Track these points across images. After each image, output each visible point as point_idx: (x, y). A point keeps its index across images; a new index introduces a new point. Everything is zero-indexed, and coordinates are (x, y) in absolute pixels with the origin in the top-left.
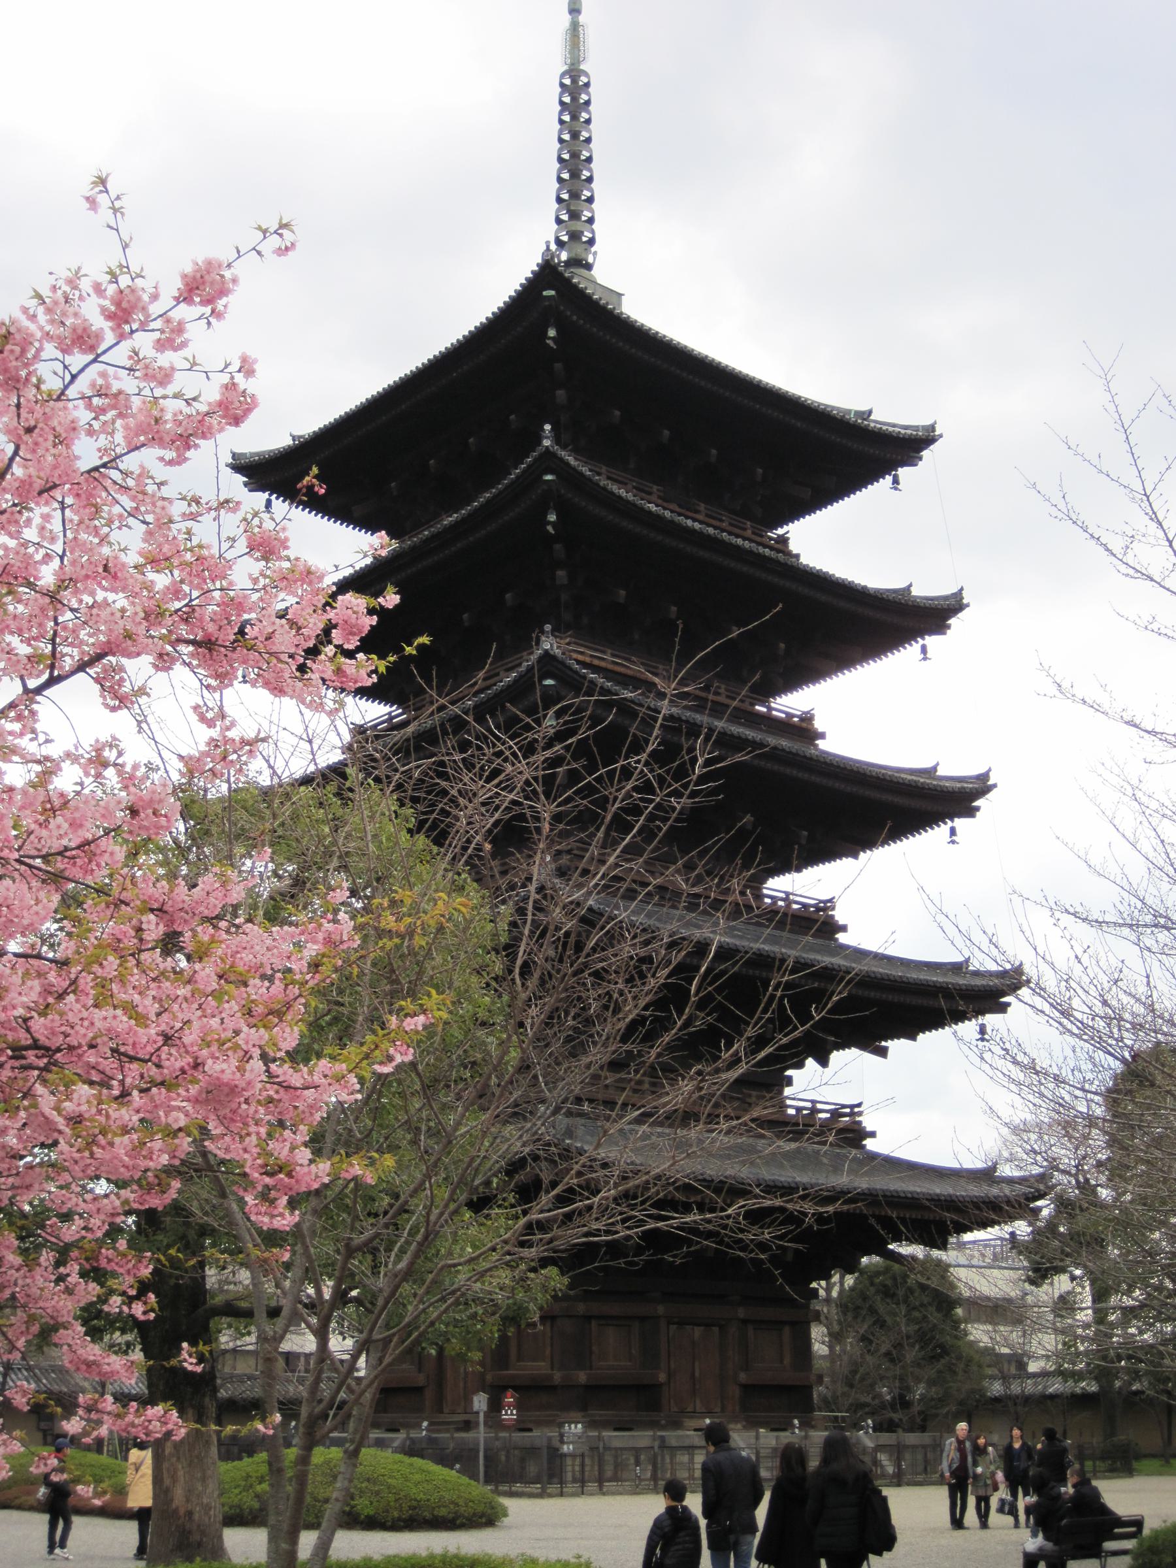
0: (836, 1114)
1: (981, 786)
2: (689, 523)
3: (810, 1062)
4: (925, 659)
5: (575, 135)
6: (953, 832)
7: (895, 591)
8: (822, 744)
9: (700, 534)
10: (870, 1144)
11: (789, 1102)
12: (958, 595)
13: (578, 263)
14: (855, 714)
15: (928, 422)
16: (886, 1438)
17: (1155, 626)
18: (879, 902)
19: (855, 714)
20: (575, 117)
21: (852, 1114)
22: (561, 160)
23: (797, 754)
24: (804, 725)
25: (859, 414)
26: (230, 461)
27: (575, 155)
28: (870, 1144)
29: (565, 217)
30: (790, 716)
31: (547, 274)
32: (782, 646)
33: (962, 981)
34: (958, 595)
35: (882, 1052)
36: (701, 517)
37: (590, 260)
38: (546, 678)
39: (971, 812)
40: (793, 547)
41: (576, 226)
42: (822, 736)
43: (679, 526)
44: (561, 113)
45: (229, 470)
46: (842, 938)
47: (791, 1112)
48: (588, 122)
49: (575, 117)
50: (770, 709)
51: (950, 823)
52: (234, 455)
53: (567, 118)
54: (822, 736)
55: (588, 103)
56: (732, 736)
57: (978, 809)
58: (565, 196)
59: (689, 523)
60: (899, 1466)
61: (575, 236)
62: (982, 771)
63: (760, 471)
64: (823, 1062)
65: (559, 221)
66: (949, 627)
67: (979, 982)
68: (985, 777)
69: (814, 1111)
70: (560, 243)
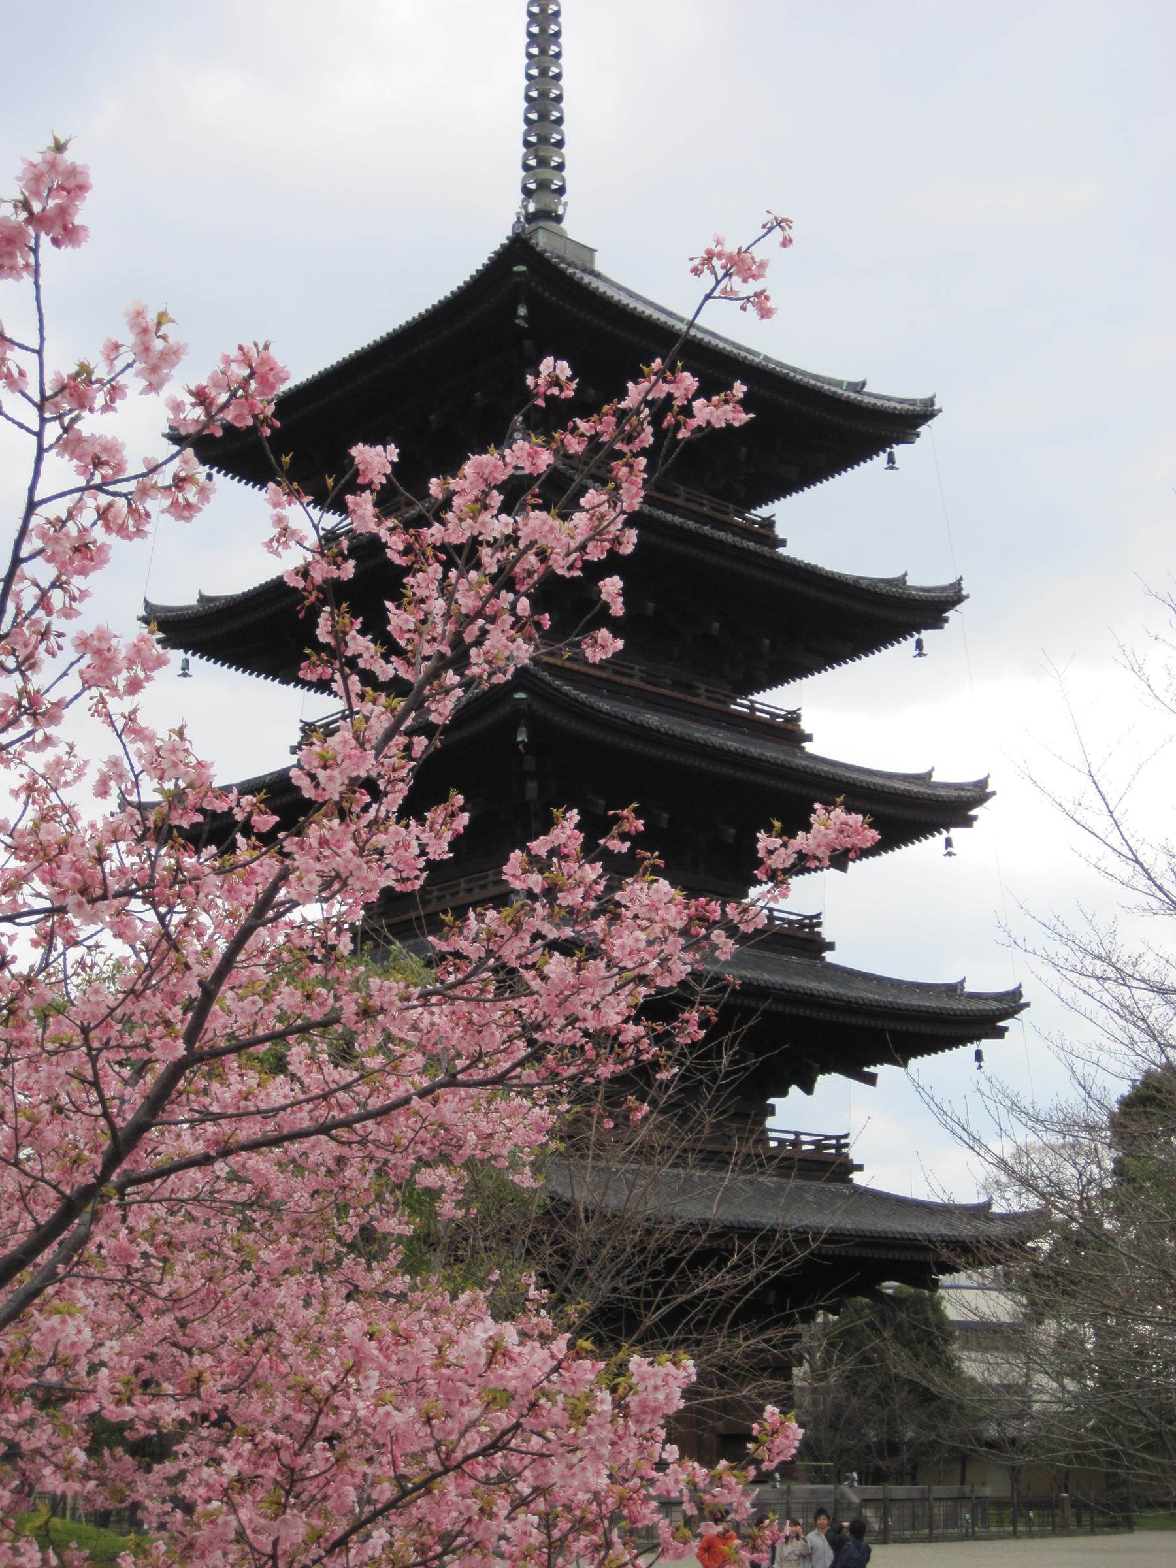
0: (819, 1145)
1: (979, 793)
2: (669, 517)
3: (794, 1090)
4: (920, 655)
5: (544, 72)
6: (949, 842)
7: (889, 581)
8: (808, 747)
9: (681, 528)
10: (857, 1178)
11: (771, 1135)
12: (957, 586)
14: (845, 715)
15: (926, 395)
16: (873, 1491)
18: (873, 916)
19: (845, 715)
20: (543, 51)
21: (839, 1147)
22: (528, 99)
24: (790, 726)
25: (849, 384)
27: (543, 94)
28: (857, 1178)
29: (533, 162)
31: (518, 248)
32: (767, 641)
33: (955, 1005)
34: (957, 586)
35: (871, 1080)
36: (679, 501)
37: (560, 211)
38: (517, 691)
39: (968, 822)
40: (780, 531)
41: (545, 174)
42: (809, 738)
43: (657, 520)
44: (529, 45)
45: (166, 441)
46: (828, 956)
47: (773, 1144)
48: (558, 55)
49: (543, 51)
50: (752, 708)
51: (945, 834)
53: (535, 51)
54: (809, 738)
55: (557, 34)
56: (714, 747)
57: (975, 818)
58: (533, 139)
59: (669, 517)
60: (886, 1522)
61: (543, 185)
63: (744, 450)
64: (808, 1089)
65: (526, 167)
66: (946, 620)
67: (974, 1006)
68: (983, 783)
69: (796, 1143)
70: (527, 192)
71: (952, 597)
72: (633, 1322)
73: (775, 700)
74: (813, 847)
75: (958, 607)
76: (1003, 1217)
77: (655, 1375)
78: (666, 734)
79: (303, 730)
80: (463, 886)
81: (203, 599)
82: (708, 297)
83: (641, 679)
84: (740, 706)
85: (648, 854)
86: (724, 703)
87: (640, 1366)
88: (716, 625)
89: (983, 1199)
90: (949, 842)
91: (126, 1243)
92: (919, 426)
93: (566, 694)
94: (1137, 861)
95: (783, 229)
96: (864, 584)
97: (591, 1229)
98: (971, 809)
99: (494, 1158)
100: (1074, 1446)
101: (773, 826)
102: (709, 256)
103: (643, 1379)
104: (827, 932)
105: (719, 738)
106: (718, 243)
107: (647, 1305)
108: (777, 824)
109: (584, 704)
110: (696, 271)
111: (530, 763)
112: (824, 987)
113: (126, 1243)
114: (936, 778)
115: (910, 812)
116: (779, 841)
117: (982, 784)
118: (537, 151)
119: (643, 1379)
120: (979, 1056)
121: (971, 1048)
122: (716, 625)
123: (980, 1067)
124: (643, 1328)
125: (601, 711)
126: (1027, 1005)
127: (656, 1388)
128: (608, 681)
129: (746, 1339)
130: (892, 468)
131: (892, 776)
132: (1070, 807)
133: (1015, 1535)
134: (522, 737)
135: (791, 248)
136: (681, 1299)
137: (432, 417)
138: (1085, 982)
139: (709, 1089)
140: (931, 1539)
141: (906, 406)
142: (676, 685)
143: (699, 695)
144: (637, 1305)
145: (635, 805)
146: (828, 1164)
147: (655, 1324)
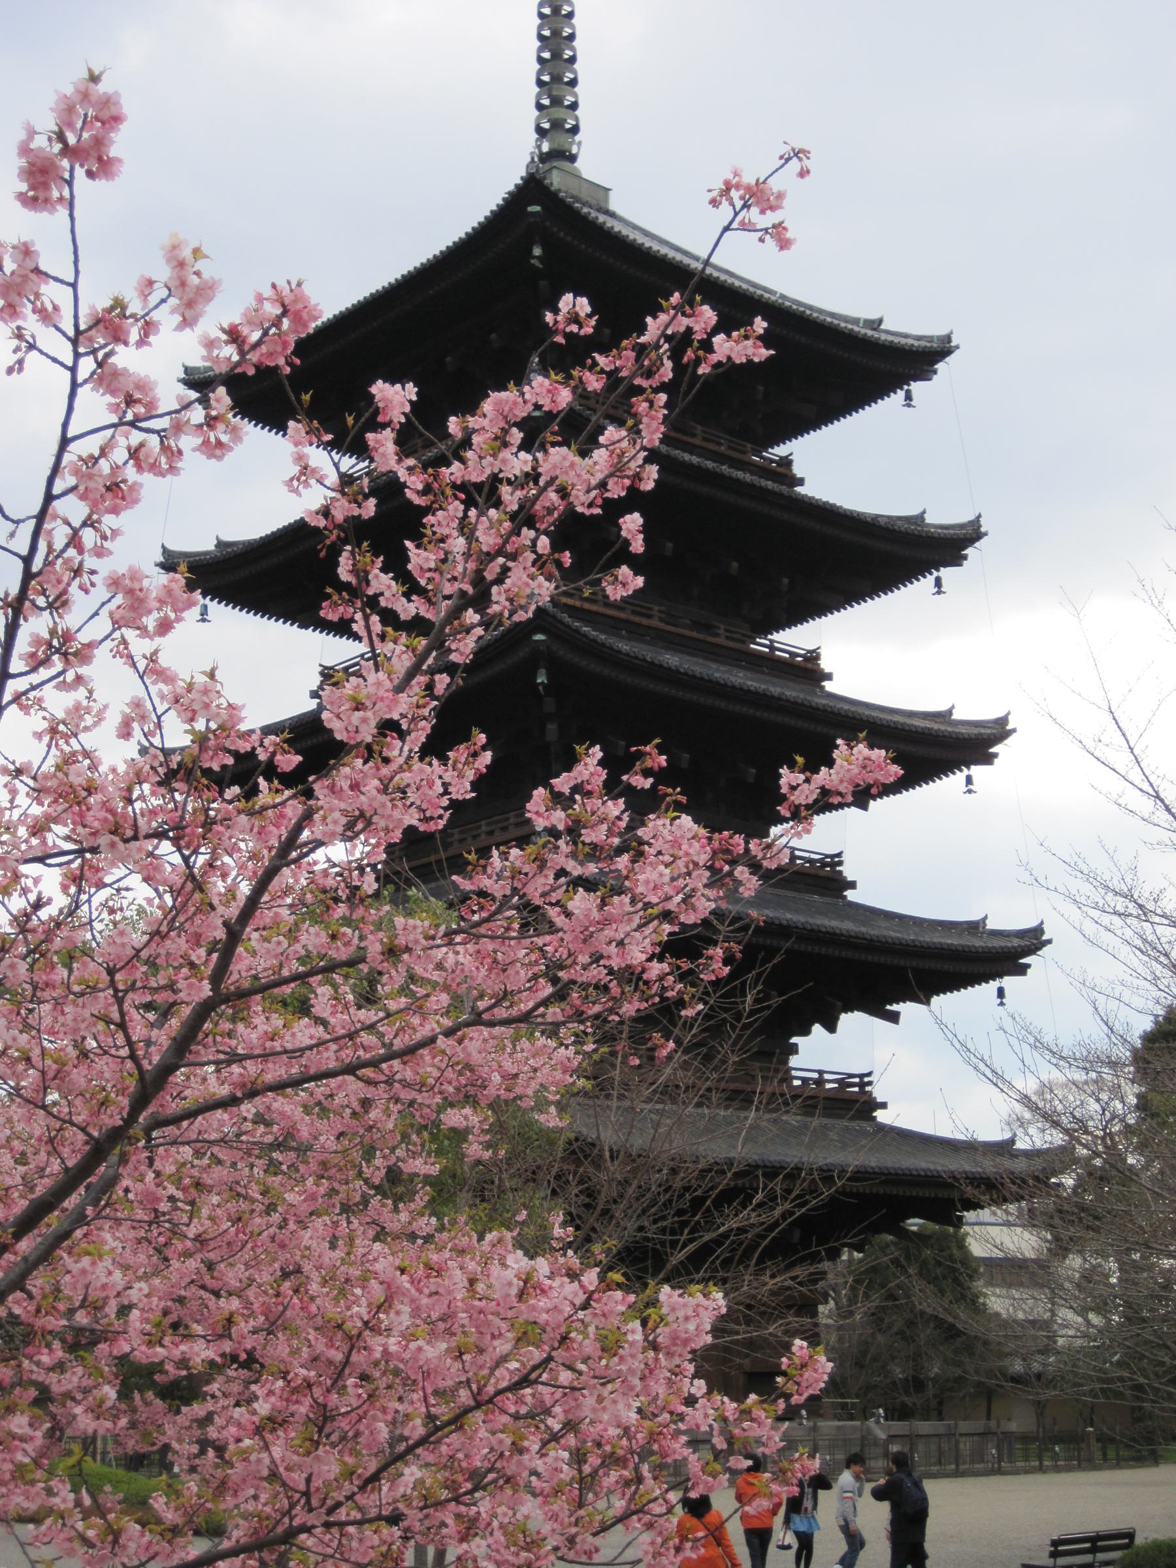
0: (843, 1083)
1: (999, 731)
2: (687, 457)
3: (817, 1029)
4: (939, 593)
6: (969, 780)
7: (907, 519)
8: (829, 686)
9: (698, 468)
10: (881, 1116)
11: (794, 1073)
13: (564, 156)
14: (864, 653)
15: (943, 332)
16: (899, 1427)
17: (1122, 801)
18: (894, 854)
21: (862, 1085)
22: (541, 37)
23: (802, 705)
24: (809, 666)
26: (183, 376)
27: (556, 33)
28: (881, 1116)
30: (793, 655)
31: (532, 188)
33: (977, 943)
35: (894, 1018)
36: (697, 441)
37: (574, 151)
38: (536, 633)
39: (988, 759)
40: (798, 470)
41: (559, 113)
42: (829, 677)
45: (181, 386)
46: (850, 895)
47: (797, 1083)
50: (771, 647)
52: (187, 370)
54: (829, 677)
56: (734, 687)
57: (995, 755)
58: (546, 78)
59: (687, 457)
61: (557, 125)
62: (1000, 714)
63: (761, 388)
64: (831, 1027)
65: (540, 107)
66: (965, 557)
67: (997, 943)
68: (1002, 721)
69: (820, 1082)
70: (541, 132)
71: (971, 534)
72: (659, 1261)
73: (794, 639)
74: (836, 782)
75: (977, 544)
76: (1027, 1154)
77: (685, 1305)
78: (686, 674)
79: (322, 674)
80: (484, 828)
81: (220, 544)
82: (727, 229)
83: (661, 620)
84: (760, 645)
85: (670, 790)
86: (744, 642)
87: (670, 1296)
88: (735, 565)
89: (1007, 1135)
90: (969, 780)
91: (153, 1187)
92: (937, 362)
93: (585, 636)
94: (1158, 797)
95: (800, 159)
96: (882, 522)
97: (616, 1170)
98: (992, 746)
99: (520, 1098)
100: (1100, 1380)
101: (795, 762)
102: (728, 187)
103: (673, 1309)
104: (848, 871)
105: (739, 678)
106: (736, 174)
107: (674, 1244)
108: (800, 760)
109: (603, 645)
110: (714, 203)
111: (549, 705)
112: (846, 926)
113: (153, 1187)
114: (957, 715)
115: (933, 749)
116: (802, 777)
117: (1002, 721)
118: (550, 90)
119: (673, 1309)
120: (1001, 993)
121: (993, 985)
122: (735, 565)
123: (1002, 1004)
124: (669, 1266)
125: (619, 652)
126: (1049, 942)
127: (687, 1319)
128: (627, 621)
129: (773, 1276)
130: (909, 405)
131: (912, 714)
132: (1090, 745)
133: (1041, 1469)
134: (541, 679)
135: (807, 179)
136: (707, 1237)
137: (448, 359)
138: (1106, 919)
139: (733, 1028)
140: (957, 1474)
141: (923, 343)
142: (696, 625)
143: (717, 635)
144: (663, 1243)
145: (657, 741)
146: (851, 1102)
147: (682, 1262)
